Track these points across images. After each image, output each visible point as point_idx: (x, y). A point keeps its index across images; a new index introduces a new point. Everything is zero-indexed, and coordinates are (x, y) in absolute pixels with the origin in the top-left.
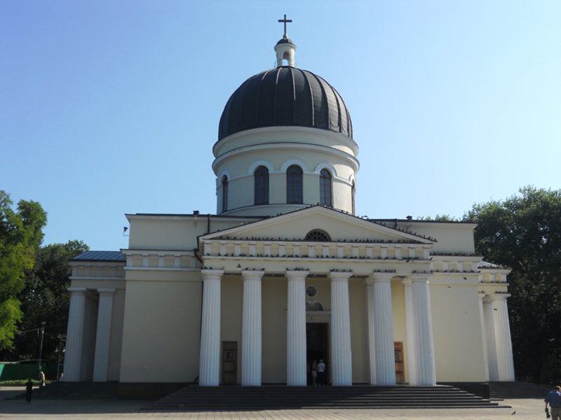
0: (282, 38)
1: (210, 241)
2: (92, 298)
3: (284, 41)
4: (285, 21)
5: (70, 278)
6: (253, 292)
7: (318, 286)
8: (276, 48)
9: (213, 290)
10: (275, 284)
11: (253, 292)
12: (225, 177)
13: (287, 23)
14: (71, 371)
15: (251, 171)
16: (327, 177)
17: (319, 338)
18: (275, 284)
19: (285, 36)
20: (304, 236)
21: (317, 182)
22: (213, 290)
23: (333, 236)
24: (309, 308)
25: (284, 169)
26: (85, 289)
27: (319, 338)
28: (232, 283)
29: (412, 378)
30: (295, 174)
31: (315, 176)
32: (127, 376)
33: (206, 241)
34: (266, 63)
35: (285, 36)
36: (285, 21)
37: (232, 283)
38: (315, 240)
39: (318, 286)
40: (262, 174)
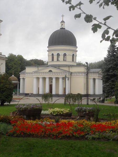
0: (62, 20)
3: (63, 22)
4: (63, 16)
7: (51, 79)
8: (61, 23)
10: (44, 79)
11: (41, 80)
14: (21, 92)
16: (65, 55)
17: (51, 86)
18: (44, 79)
19: (63, 20)
20: (48, 71)
21: (63, 56)
22: (35, 80)
27: (51, 86)
28: (38, 79)
30: (58, 55)
31: (62, 55)
32: (26, 92)
34: (57, 27)
35: (63, 20)
36: (63, 16)
39: (51, 79)
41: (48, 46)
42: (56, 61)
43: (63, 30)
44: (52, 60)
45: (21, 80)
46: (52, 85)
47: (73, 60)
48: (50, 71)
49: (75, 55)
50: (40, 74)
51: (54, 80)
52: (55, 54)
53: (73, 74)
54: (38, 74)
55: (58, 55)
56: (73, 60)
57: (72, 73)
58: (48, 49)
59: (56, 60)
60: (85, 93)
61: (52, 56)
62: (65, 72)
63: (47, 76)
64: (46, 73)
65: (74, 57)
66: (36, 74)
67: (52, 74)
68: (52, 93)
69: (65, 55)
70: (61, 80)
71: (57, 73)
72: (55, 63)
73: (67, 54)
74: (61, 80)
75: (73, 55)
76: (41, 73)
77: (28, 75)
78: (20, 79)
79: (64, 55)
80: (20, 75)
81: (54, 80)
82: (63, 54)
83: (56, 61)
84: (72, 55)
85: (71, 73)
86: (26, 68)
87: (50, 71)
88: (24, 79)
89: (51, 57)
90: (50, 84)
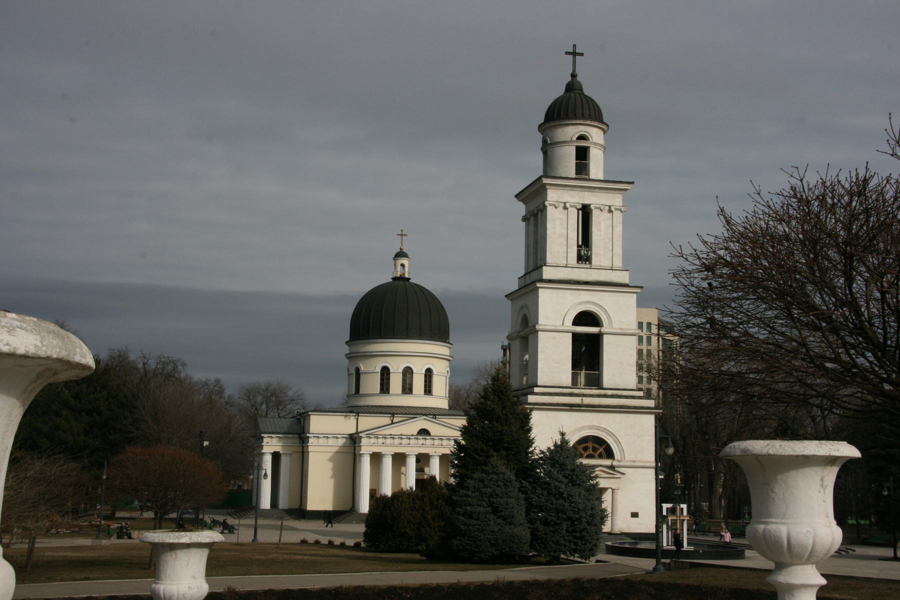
0: (399, 250)
1: (365, 436)
2: (276, 456)
4: (402, 235)
5: (263, 444)
6: (388, 463)
9: (366, 464)
10: (399, 459)
11: (388, 463)
12: (358, 370)
13: (404, 237)
14: (266, 503)
15: (379, 370)
16: (429, 373)
18: (399, 459)
20: (415, 433)
23: (432, 434)
24: (417, 470)
25: (401, 370)
28: (376, 458)
30: (408, 373)
33: (363, 436)
36: (402, 235)
37: (376, 458)
40: (385, 372)
41: (348, 339)
42: (397, 395)
43: (401, 282)
44: (425, 391)
48: (424, 432)
54: (381, 441)
58: (346, 349)
59: (400, 391)
61: (382, 375)
63: (412, 450)
67: (429, 442)
69: (429, 373)
72: (396, 398)
73: (435, 372)
76: (392, 437)
77: (322, 441)
83: (397, 395)
86: (312, 417)
87: (424, 432)
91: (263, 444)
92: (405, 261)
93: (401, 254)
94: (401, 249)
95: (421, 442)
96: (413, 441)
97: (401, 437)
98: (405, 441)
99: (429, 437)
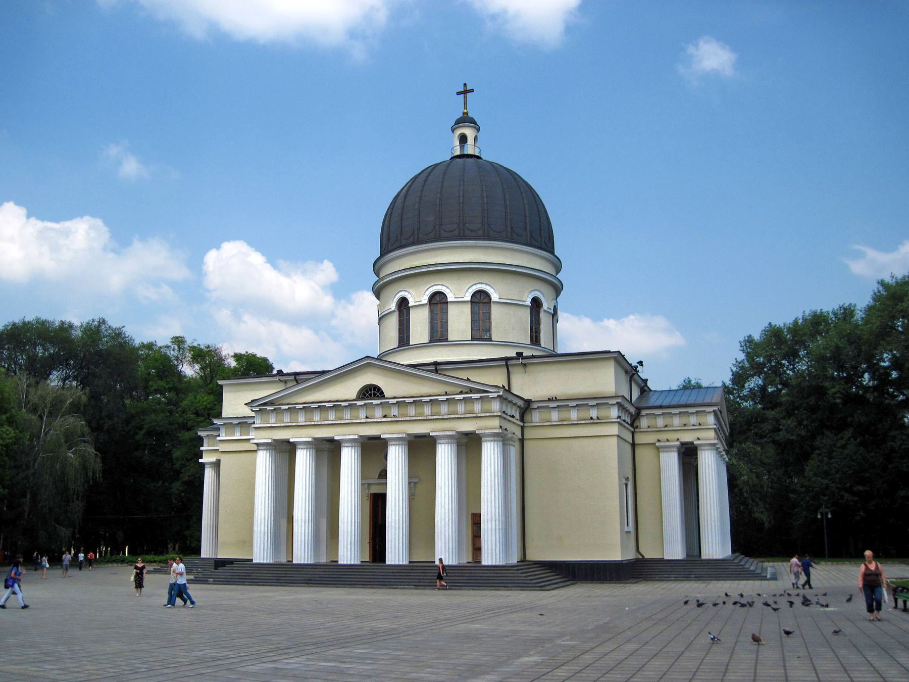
3: (465, 120)
6: (304, 460)
16: (480, 300)
20: (354, 396)
21: (467, 309)
22: (264, 462)
23: (386, 395)
25: (425, 300)
26: (215, 461)
29: (488, 559)
30: (438, 301)
36: (465, 92)
38: (370, 397)
45: (209, 474)
46: (383, 496)
47: (535, 339)
49: (546, 305)
50: (301, 419)
51: (396, 458)
52: (418, 295)
53: (536, 417)
54: (287, 419)
55: (438, 301)
56: (535, 339)
57: (528, 402)
59: (425, 339)
60: (631, 555)
61: (400, 316)
62: (479, 391)
64: (337, 406)
65: (545, 320)
66: (272, 420)
67: (378, 413)
68: (383, 559)
69: (480, 300)
70: (445, 456)
71: (417, 403)
73: (495, 297)
74: (445, 456)
75: (536, 304)
76: (307, 409)
78: (202, 466)
79: (472, 302)
80: (200, 441)
81: (396, 458)
82: (468, 298)
84: (528, 303)
85: (527, 406)
87: (371, 392)
88: (217, 465)
89: (393, 323)
90: (375, 490)
91: (201, 448)
92: (469, 133)
93: (465, 120)
94: (464, 113)
95: (362, 414)
96: (347, 416)
97: (322, 408)
98: (331, 416)
99: (378, 402)
